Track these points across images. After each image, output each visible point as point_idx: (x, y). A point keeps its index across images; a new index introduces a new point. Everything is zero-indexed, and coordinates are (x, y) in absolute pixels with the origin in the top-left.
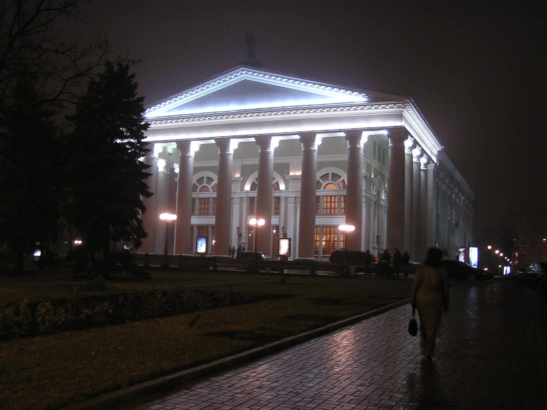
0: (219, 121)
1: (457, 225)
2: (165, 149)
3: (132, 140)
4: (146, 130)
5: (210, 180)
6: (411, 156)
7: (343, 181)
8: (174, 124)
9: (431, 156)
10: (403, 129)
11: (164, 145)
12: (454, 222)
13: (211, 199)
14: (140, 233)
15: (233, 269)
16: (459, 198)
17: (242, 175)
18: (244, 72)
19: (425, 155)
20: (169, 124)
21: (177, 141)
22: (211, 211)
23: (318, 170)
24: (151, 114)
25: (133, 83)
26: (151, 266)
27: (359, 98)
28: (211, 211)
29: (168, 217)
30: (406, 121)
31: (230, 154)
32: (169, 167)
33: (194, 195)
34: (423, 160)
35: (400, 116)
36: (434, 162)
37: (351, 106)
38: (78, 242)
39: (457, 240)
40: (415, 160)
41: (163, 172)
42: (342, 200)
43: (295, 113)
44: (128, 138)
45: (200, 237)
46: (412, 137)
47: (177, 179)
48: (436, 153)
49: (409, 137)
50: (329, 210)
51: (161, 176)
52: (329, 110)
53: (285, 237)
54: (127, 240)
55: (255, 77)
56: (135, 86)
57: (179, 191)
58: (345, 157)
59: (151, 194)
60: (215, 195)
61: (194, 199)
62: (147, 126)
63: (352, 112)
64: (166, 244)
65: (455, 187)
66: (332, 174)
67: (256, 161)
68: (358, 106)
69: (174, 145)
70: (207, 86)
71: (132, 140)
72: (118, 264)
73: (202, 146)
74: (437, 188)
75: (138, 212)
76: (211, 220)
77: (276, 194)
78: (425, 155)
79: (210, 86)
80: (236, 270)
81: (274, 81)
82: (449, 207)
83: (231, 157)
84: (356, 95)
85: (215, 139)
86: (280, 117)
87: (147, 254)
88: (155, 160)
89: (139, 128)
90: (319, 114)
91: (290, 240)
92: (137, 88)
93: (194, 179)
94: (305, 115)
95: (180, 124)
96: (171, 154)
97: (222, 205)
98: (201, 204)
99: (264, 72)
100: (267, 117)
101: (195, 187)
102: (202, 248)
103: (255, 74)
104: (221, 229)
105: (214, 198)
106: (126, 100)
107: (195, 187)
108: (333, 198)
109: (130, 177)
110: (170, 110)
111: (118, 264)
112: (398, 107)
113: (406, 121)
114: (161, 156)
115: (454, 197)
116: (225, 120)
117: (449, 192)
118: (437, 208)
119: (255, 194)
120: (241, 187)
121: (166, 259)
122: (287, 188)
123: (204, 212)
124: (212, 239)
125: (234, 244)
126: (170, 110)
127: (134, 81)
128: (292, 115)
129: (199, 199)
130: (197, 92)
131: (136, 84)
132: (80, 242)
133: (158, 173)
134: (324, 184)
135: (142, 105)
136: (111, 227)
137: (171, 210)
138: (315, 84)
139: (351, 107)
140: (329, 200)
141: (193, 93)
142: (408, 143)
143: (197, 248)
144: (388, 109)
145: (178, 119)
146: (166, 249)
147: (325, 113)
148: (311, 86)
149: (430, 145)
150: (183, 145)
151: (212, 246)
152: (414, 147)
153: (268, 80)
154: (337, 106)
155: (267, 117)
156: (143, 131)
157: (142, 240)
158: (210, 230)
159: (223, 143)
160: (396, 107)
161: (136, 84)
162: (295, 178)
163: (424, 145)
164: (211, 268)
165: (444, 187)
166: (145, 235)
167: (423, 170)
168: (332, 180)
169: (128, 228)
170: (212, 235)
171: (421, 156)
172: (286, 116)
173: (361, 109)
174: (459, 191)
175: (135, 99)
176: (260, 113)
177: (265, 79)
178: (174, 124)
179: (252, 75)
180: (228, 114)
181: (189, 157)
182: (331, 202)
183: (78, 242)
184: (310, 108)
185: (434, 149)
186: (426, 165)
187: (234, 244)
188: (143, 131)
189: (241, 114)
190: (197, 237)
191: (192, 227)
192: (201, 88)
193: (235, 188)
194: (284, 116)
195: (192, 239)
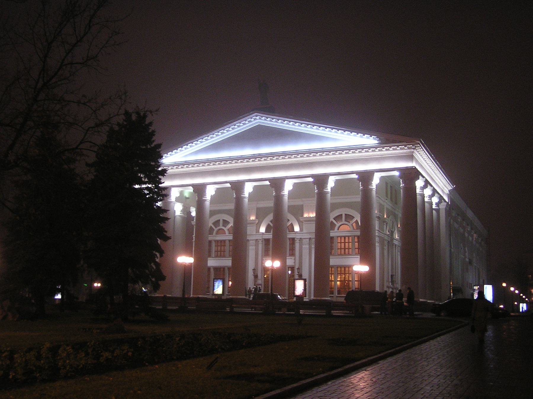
0: (234, 165)
1: (470, 262)
2: (181, 193)
3: (150, 186)
4: (163, 175)
5: (226, 223)
6: (423, 196)
7: (357, 222)
8: (191, 169)
9: (442, 195)
10: (414, 169)
11: (181, 189)
12: (467, 260)
13: (227, 243)
14: (158, 277)
15: (248, 310)
16: (472, 236)
17: (257, 218)
18: (258, 118)
19: (436, 195)
20: (185, 169)
21: (193, 186)
22: (227, 253)
23: (331, 211)
24: (169, 159)
25: (150, 131)
26: (169, 308)
27: (370, 140)
28: (227, 253)
29: (185, 260)
30: (417, 161)
31: (245, 197)
32: (186, 211)
33: (210, 238)
34: (435, 200)
35: (411, 157)
36: (446, 202)
37: (362, 148)
38: (97, 285)
39: (471, 277)
40: (426, 199)
41: (180, 216)
42: (356, 240)
43: (307, 156)
44: (146, 184)
45: (216, 279)
46: (423, 177)
47: (194, 222)
48: (448, 192)
49: (421, 177)
51: (178, 219)
52: (340, 153)
53: (300, 278)
54: (145, 284)
55: (269, 122)
56: (153, 134)
57: (196, 233)
58: (358, 198)
59: (169, 238)
60: (231, 238)
61: (210, 242)
62: (164, 172)
63: (364, 154)
64: (184, 286)
65: (468, 225)
67: (270, 204)
68: (369, 148)
69: (191, 189)
70: (222, 131)
71: (150, 186)
72: (137, 307)
73: (218, 190)
74: (449, 226)
75: (156, 255)
76: (227, 262)
77: (290, 235)
78: (436, 195)
79: (225, 131)
80: (253, 311)
81: (287, 126)
82: (462, 245)
83: (246, 200)
84: (367, 138)
85: (231, 183)
86: (293, 160)
87: (165, 296)
88: (172, 204)
89: (156, 174)
90: (331, 157)
91: (305, 280)
92: (154, 135)
93: (210, 222)
94: (318, 158)
95: (196, 168)
96: (188, 198)
97: (238, 247)
98: (218, 246)
99: (277, 118)
100: (281, 161)
101: (211, 230)
102: (218, 289)
103: (269, 119)
104: (237, 271)
105: (230, 241)
106: (144, 147)
107: (211, 230)
108: (347, 238)
109: (147, 221)
110: (186, 156)
111: (137, 307)
112: (409, 148)
113: (417, 161)
114: (178, 200)
115: (466, 235)
116: (240, 164)
117: (461, 230)
118: (451, 247)
119: (270, 236)
120: (256, 230)
121: (184, 301)
122: (301, 229)
123: (220, 254)
124: (229, 281)
125: (250, 285)
126: (186, 156)
127: (152, 128)
128: (305, 159)
129: (215, 241)
130: (212, 138)
131: (154, 131)
132: (99, 285)
133: (175, 217)
134: (338, 225)
135: (159, 152)
136: (130, 270)
137: (188, 252)
138: (326, 128)
139: (363, 149)
140: (343, 241)
141: (209, 138)
142: (419, 183)
143: (214, 290)
144: (399, 150)
145: (194, 164)
146: (184, 291)
147: (338, 156)
148: (323, 130)
149: (441, 185)
150: (199, 190)
151: (229, 287)
152: (425, 187)
153: (281, 124)
154: (349, 149)
155: (281, 161)
156: (160, 177)
157: (161, 283)
158: (227, 271)
159: (238, 186)
160: (406, 148)
161: (154, 131)
162: (309, 220)
163: (435, 185)
164: (228, 309)
165: (456, 225)
166: (163, 278)
167: (435, 209)
168: (346, 221)
169: (147, 271)
170: (229, 277)
171: (433, 195)
172: (299, 159)
173: (373, 151)
174: (472, 229)
175: (152, 146)
176: (273, 157)
177: (278, 124)
178: (191, 169)
179: (265, 120)
180: (242, 158)
181: (205, 200)
182: (345, 243)
183: (97, 285)
184: (322, 151)
185: (446, 188)
186: (437, 204)
187: (250, 285)
188: (160, 177)
189: (256, 158)
190: (214, 279)
191: (209, 269)
192: (217, 134)
193: (250, 230)
194: (298, 159)
195: (209, 281)
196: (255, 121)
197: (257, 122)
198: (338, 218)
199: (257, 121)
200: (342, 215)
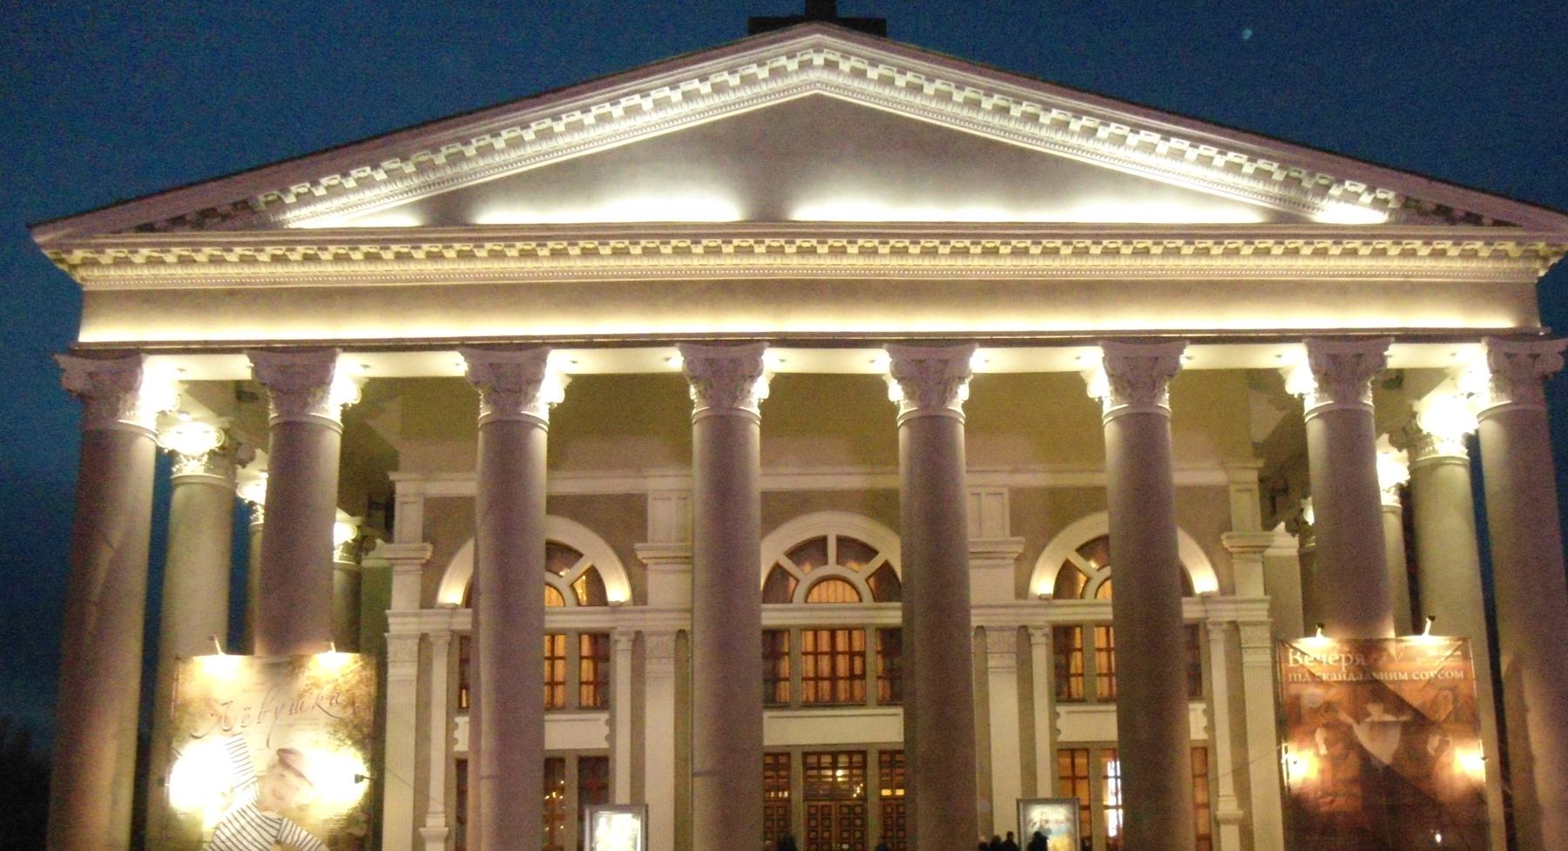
50: (826, 685)
66: (842, 541)
108: (856, 634)
122: (639, 596)
140: (824, 645)
182: (833, 653)
196: (804, 77)
197: (811, 84)
198: (811, 550)
199: (812, 76)
200: (822, 541)
